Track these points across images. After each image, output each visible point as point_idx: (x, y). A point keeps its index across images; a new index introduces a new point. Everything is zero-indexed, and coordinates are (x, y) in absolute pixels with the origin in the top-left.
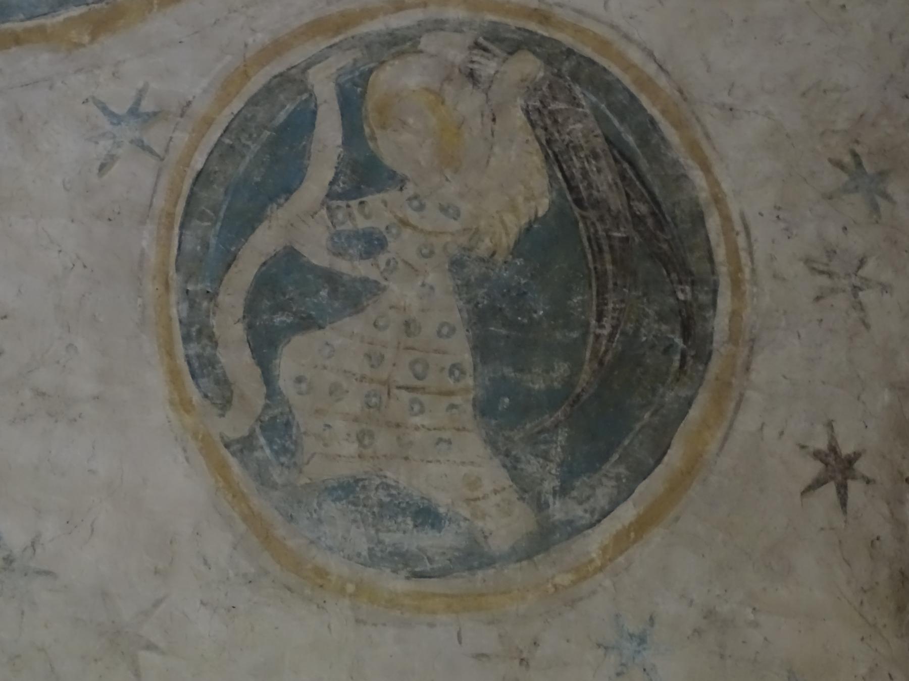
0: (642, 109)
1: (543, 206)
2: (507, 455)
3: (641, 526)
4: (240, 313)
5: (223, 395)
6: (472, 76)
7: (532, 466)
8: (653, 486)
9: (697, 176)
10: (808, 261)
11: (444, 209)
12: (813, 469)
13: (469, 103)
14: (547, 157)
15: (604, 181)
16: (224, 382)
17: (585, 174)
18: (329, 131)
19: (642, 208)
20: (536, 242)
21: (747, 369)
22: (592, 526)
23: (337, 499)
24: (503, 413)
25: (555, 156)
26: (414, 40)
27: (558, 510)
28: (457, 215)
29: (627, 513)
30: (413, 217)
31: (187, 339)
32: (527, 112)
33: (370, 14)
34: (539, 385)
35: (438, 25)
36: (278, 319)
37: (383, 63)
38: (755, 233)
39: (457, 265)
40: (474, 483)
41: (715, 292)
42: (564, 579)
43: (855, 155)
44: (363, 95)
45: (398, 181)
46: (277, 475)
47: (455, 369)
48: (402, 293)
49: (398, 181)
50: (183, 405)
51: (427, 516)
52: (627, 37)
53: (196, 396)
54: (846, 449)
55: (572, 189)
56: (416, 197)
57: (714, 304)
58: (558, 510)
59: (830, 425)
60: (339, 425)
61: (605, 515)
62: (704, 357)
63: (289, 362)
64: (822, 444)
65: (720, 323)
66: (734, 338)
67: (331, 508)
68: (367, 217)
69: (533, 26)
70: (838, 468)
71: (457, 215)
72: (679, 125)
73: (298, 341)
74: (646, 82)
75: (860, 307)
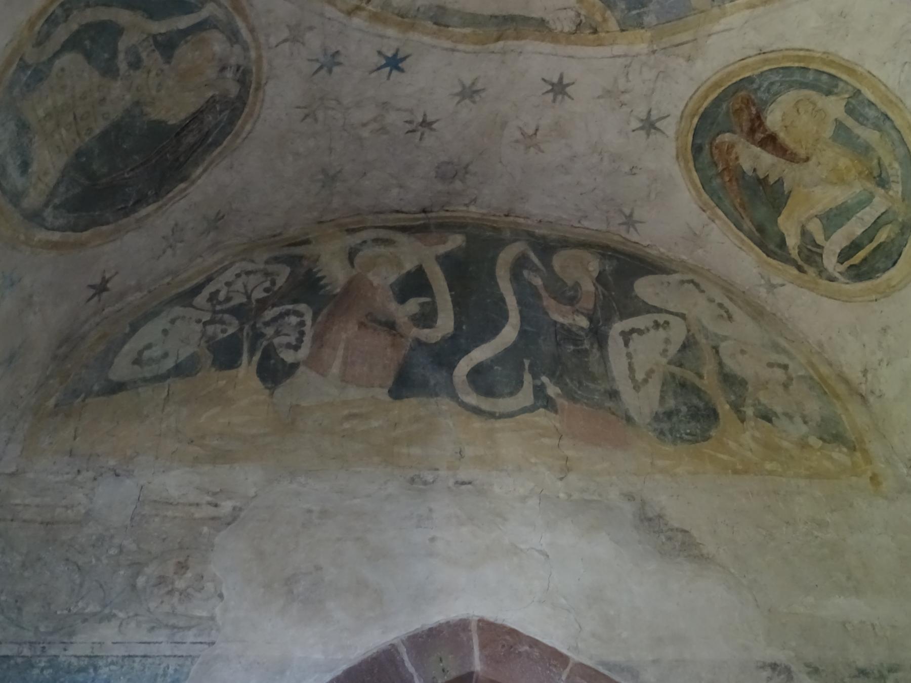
0: (224, 138)
1: (172, 122)
2: (63, 176)
3: (55, 246)
4: (84, 22)
5: (41, 41)
6: (223, 69)
7: (62, 189)
8: (72, 236)
9: (200, 170)
10: (176, 225)
11: (159, 84)
12: (97, 281)
13: (211, 73)
14: (194, 114)
15: (190, 139)
16: (48, 35)
17: (192, 131)
18: (184, 22)
19: (182, 159)
20: (158, 130)
21: (127, 232)
22: (47, 229)
23: (17, 125)
24: (80, 162)
25: (196, 117)
26: (237, 42)
27: (48, 213)
28: (158, 91)
29: (56, 236)
30: (153, 74)
31: (62, 5)
32: (212, 97)
33: (245, 18)
34: (95, 167)
35: (246, 49)
36: (87, 43)
37: (223, 32)
38: (182, 201)
39: (137, 103)
40: (46, 173)
41: (154, 202)
42: (22, 237)
43: (223, 217)
44: (205, 30)
45: (168, 59)
46: (16, 91)
47: (90, 130)
48: (117, 88)
49: (168, 59)
50: (31, 24)
51: (25, 166)
52: (255, 123)
53: (37, 28)
54: (109, 285)
55: (183, 129)
56: (162, 71)
57: (148, 205)
58: (48, 213)
59: (117, 273)
60: (49, 102)
61: (53, 229)
62: (127, 215)
63: (67, 59)
64: (107, 276)
65: (143, 212)
66: (138, 221)
67: (12, 126)
68: (148, 56)
69: (253, 86)
70: (101, 288)
71: (158, 91)
72: (220, 153)
73: (80, 57)
74: (237, 135)
75: (164, 252)
